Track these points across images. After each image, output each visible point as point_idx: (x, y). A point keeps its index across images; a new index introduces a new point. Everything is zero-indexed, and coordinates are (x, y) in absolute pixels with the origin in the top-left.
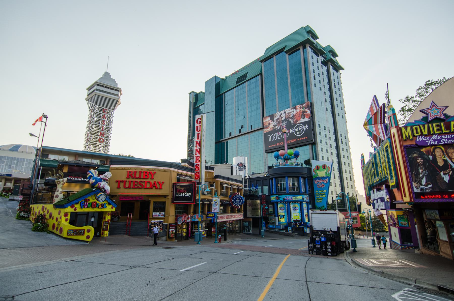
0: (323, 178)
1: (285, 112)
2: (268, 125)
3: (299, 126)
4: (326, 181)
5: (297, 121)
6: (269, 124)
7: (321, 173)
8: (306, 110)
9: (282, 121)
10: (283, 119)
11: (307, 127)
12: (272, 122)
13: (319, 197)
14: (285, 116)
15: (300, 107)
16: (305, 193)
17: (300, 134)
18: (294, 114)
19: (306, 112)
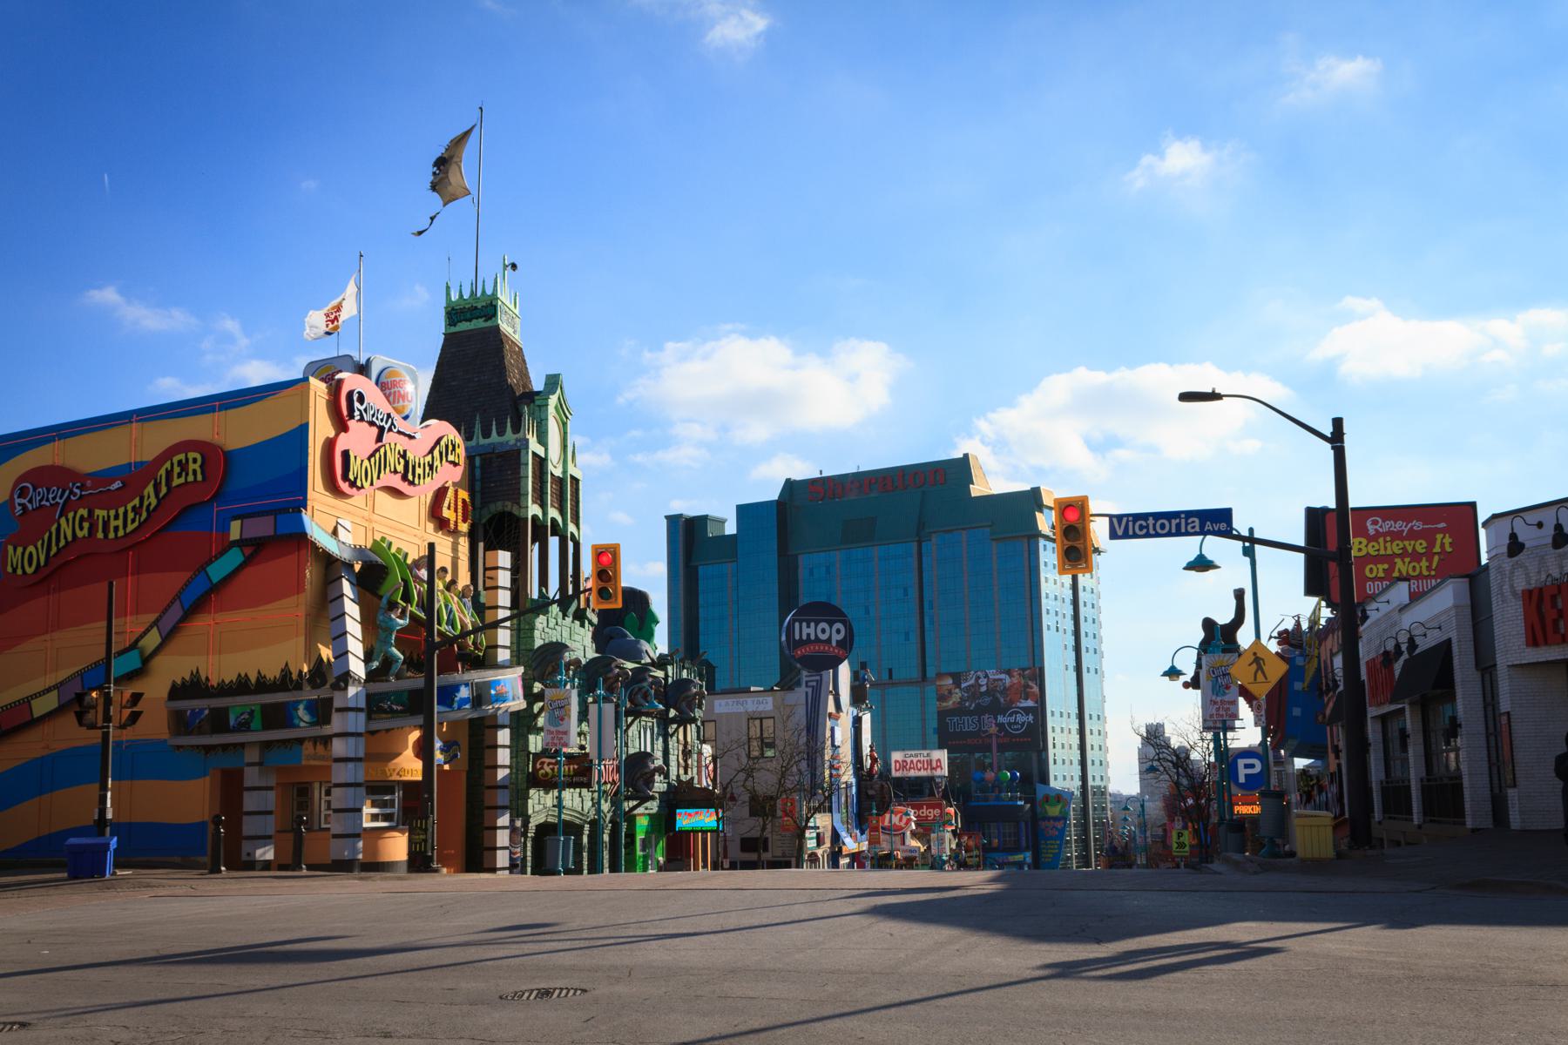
0: (1056, 819)
1: (986, 676)
2: (946, 693)
3: (1017, 713)
4: (1059, 825)
5: (1012, 702)
6: (950, 692)
7: (1054, 811)
8: (1030, 683)
9: (981, 693)
10: (984, 689)
11: (1031, 718)
12: (957, 690)
13: (1047, 853)
14: (987, 684)
15: (1020, 674)
16: (1027, 849)
17: (1018, 730)
18: (1007, 685)
19: (1032, 688)
